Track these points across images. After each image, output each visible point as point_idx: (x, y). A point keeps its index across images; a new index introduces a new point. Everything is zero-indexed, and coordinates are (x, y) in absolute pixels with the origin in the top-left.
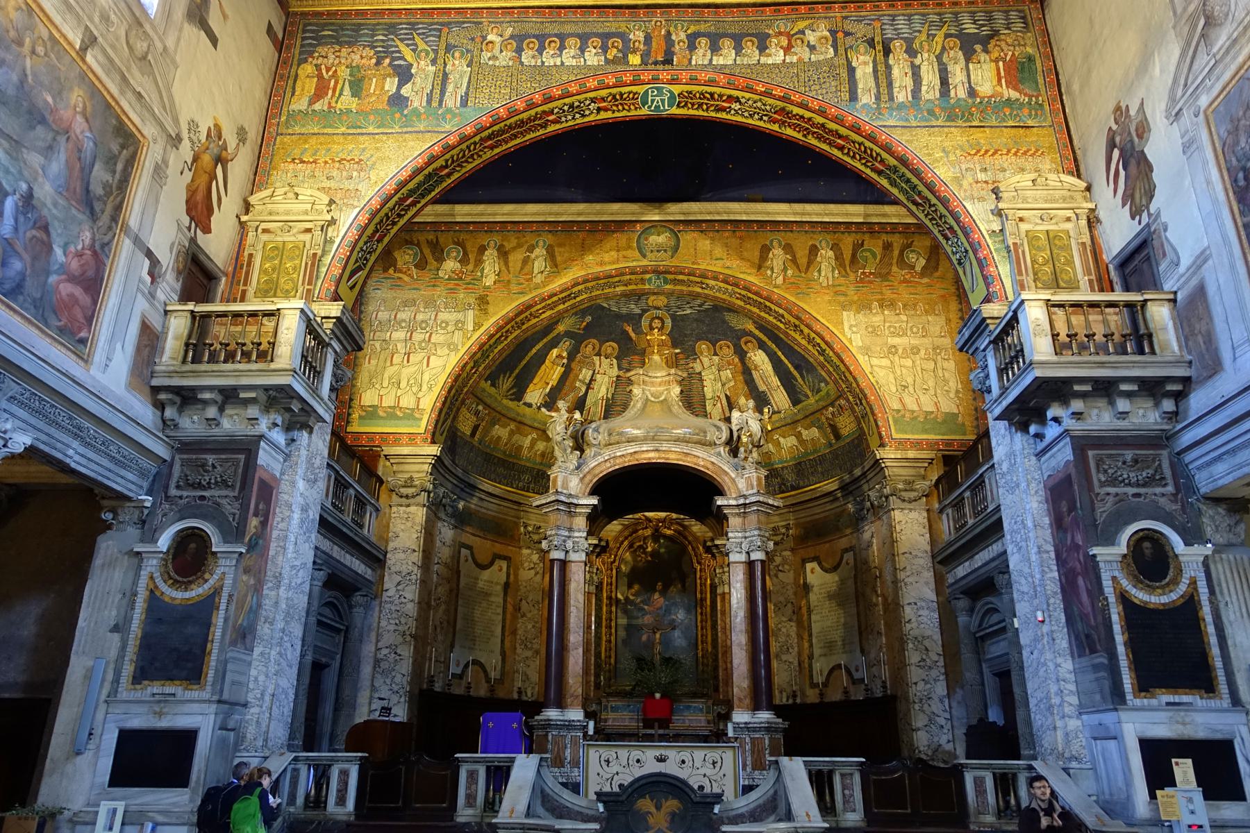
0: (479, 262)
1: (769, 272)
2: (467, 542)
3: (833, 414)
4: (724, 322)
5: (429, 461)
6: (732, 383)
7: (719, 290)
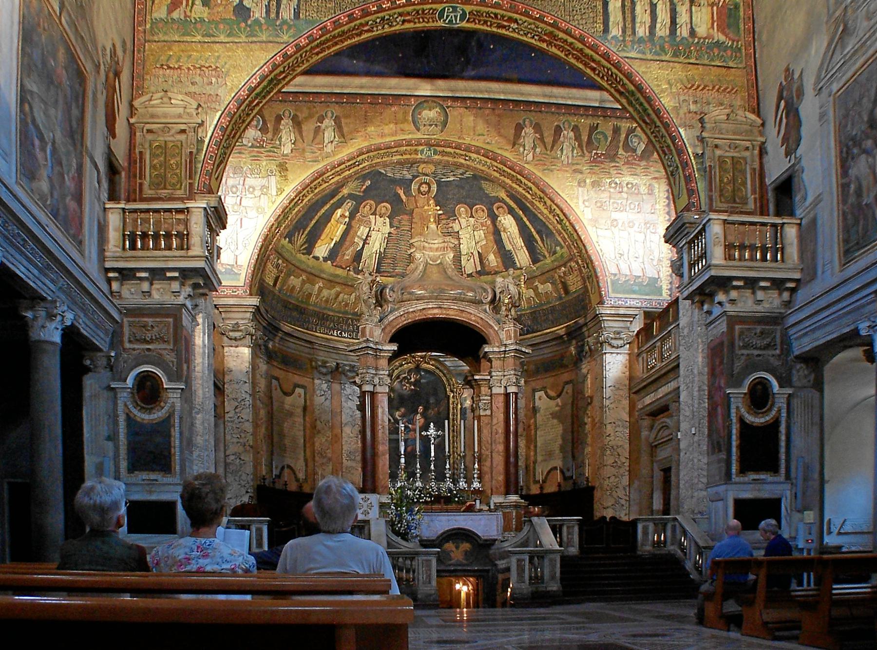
0: (277, 130)
1: (521, 149)
4: (481, 189)
7: (480, 162)
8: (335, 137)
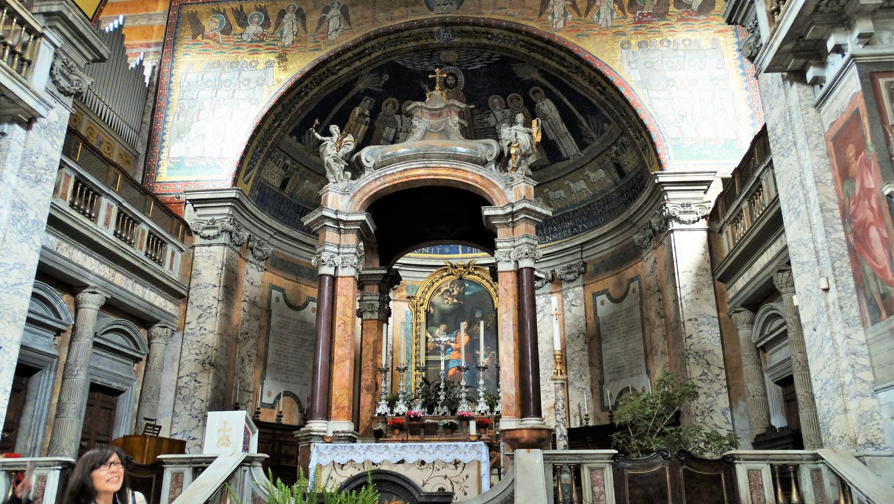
0: (278, 24)
1: (550, 18)
2: (278, 285)
3: (617, 153)
5: (230, 204)
8: (340, 25)
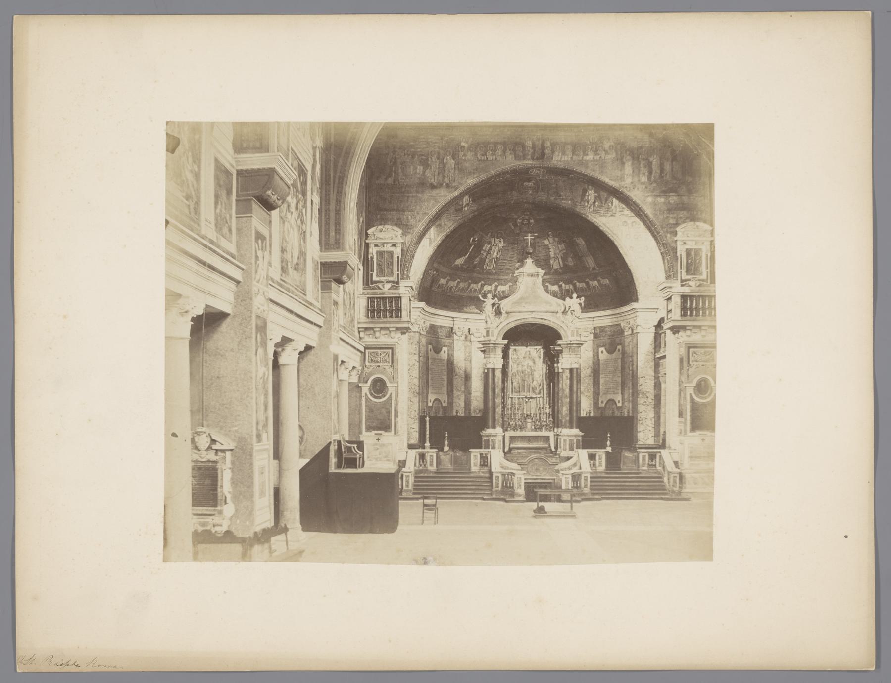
6: (564, 251)
